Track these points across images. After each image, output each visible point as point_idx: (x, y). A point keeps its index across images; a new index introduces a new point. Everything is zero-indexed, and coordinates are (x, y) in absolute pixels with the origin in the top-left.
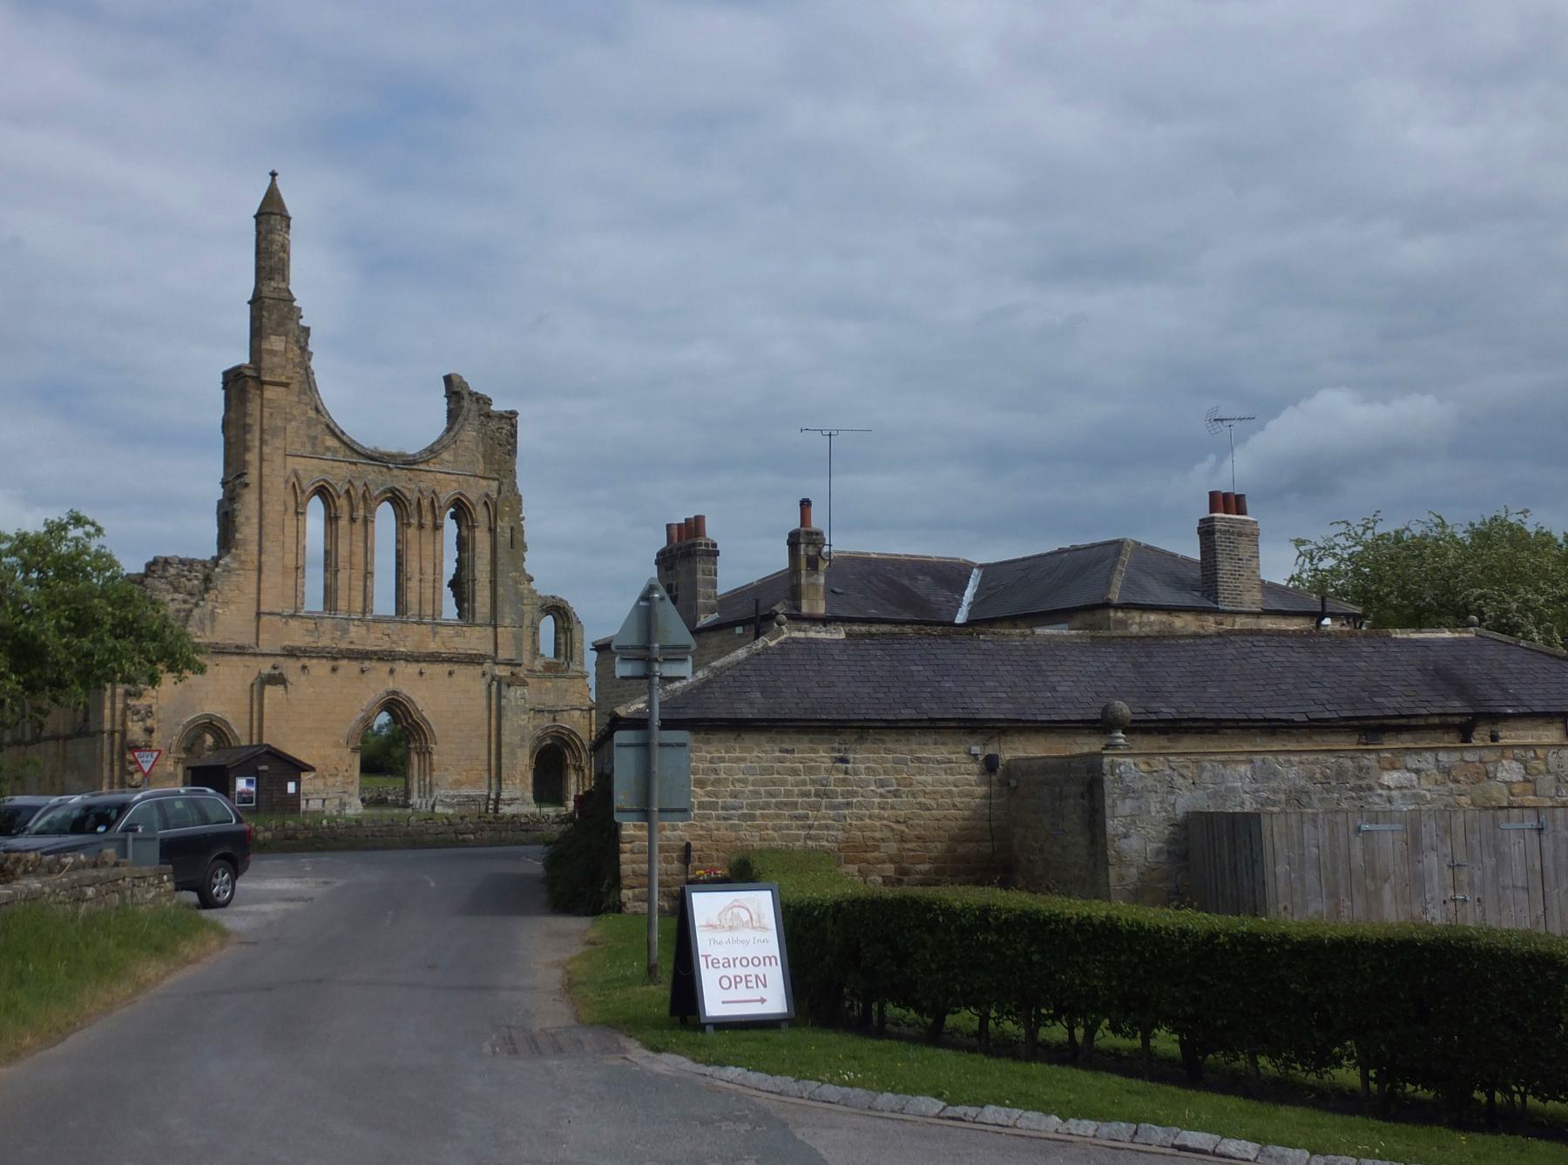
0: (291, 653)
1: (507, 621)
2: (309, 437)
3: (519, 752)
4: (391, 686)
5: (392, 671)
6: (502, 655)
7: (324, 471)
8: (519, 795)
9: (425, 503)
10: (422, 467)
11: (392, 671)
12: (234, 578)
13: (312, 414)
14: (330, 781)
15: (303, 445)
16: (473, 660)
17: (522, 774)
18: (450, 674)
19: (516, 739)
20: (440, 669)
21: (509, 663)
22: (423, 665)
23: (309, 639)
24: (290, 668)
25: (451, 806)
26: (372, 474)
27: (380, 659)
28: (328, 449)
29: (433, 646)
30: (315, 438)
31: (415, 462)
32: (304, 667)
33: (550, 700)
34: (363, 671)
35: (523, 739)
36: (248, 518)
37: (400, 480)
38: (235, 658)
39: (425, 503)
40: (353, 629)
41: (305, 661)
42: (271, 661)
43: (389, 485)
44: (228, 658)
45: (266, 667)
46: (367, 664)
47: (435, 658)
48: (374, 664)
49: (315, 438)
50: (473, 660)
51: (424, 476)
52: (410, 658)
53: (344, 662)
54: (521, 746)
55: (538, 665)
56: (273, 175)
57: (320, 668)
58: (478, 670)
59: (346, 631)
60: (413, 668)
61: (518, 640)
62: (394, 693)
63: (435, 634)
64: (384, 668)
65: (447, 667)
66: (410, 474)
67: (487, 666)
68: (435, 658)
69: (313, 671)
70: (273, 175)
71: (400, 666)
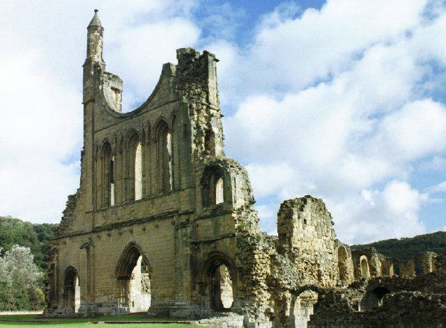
0: (96, 230)
3: (184, 272)
4: (131, 239)
10: (144, 111)
11: (131, 232)
13: (102, 108)
20: (150, 226)
21: (187, 213)
23: (103, 221)
24: (94, 236)
26: (125, 126)
35: (186, 265)
39: (146, 130)
40: (119, 211)
45: (86, 239)
47: (152, 219)
52: (140, 222)
53: (113, 231)
54: (186, 269)
56: (96, 11)
57: (104, 235)
58: (171, 220)
59: (116, 214)
62: (132, 244)
63: (153, 203)
65: (156, 222)
68: (152, 219)
70: (96, 11)
71: (137, 229)
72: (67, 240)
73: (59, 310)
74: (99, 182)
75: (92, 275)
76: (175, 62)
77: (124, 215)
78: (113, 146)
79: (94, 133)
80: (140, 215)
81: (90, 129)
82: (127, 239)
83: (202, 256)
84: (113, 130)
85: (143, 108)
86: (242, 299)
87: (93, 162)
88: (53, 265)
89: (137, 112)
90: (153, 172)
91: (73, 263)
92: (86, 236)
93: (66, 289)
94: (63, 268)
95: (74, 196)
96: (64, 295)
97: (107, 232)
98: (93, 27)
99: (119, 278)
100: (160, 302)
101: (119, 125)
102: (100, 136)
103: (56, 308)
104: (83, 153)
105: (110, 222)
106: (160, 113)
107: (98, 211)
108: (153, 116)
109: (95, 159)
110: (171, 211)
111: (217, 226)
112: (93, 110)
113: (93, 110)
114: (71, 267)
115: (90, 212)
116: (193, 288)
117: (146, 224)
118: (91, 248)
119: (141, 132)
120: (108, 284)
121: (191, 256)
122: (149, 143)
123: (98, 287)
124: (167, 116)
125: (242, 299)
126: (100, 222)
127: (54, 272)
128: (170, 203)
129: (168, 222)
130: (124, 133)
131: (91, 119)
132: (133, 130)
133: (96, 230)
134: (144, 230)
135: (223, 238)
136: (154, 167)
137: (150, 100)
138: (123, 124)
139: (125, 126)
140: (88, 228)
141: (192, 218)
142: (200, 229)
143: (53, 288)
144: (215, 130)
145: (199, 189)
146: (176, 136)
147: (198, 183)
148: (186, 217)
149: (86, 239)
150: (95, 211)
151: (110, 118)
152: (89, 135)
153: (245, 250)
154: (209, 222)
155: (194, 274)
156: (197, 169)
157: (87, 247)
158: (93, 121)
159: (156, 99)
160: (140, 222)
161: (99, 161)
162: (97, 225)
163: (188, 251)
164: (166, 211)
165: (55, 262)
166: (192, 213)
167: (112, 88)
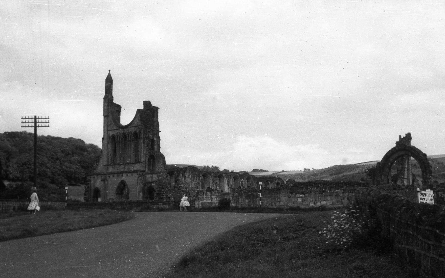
11: (122, 176)
16: (135, 171)
26: (121, 131)
45: (103, 177)
52: (126, 172)
56: (110, 71)
57: (111, 176)
70: (110, 71)
76: (142, 108)
84: (116, 131)
89: (127, 127)
94: (93, 188)
98: (109, 80)
99: (117, 194)
102: (111, 133)
104: (103, 139)
109: (108, 143)
114: (97, 188)
124: (138, 131)
126: (111, 170)
128: (137, 167)
141: (144, 173)
144: (155, 139)
149: (103, 177)
150: (108, 165)
152: (106, 132)
154: (150, 176)
155: (144, 194)
157: (104, 180)
161: (110, 144)
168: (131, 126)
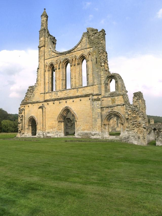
0: (46, 101)
1: (96, 83)
2: (49, 54)
3: (98, 120)
4: (66, 105)
5: (66, 102)
6: (95, 93)
7: (52, 60)
8: (97, 132)
9: (74, 59)
11: (66, 102)
12: (37, 88)
14: (54, 129)
15: (48, 56)
16: (86, 96)
17: (99, 126)
18: (81, 100)
19: (97, 116)
20: (78, 99)
21: (97, 95)
22: (73, 99)
23: (50, 97)
24: (45, 104)
25: (80, 135)
26: (62, 58)
27: (63, 99)
28: (53, 55)
29: (77, 94)
30: (50, 54)
31: (71, 51)
32: (48, 104)
33: (110, 104)
34: (60, 103)
35: (99, 116)
36: (39, 75)
37: (68, 56)
38: (36, 104)
40: (59, 93)
41: (48, 103)
42: (42, 103)
43: (65, 58)
44: (35, 104)
45: (40, 105)
46: (61, 101)
47: (77, 97)
48: (62, 101)
49: (50, 54)
50: (86, 96)
51: (74, 53)
52: (71, 98)
53: (56, 101)
55: (107, 94)
57: (51, 103)
58: (88, 98)
59: (57, 94)
60: (71, 100)
61: (100, 89)
62: (66, 107)
63: (78, 91)
64: (64, 101)
65: (80, 98)
66: (70, 54)
67: (90, 97)
68: (77, 97)
69: (50, 104)
72: (30, 105)
73: (25, 135)
74: (47, 81)
75: (44, 120)
77: (61, 95)
78: (55, 66)
79: (44, 60)
80: (71, 95)
81: (43, 58)
82: (63, 105)
83: (105, 113)
84: (56, 59)
85: (72, 50)
86: (128, 131)
87: (44, 72)
88: (22, 115)
89: (69, 52)
90: (77, 77)
91: (32, 115)
92: (40, 103)
93: (29, 126)
95: (33, 86)
96: (28, 128)
97: (52, 102)
99: (59, 122)
100: (82, 132)
101: (59, 57)
102: (48, 62)
103: (23, 133)
105: (53, 97)
106: (81, 53)
107: (47, 93)
108: (78, 54)
109: (45, 71)
110: (87, 94)
111: (113, 101)
112: (44, 50)
113: (44, 50)
115: (43, 93)
116: (102, 126)
117: (74, 99)
118: (44, 109)
119: (71, 60)
120: (53, 124)
121: (101, 113)
122: (75, 65)
123: (47, 126)
125: (128, 131)
126: (48, 97)
127: (22, 118)
129: (87, 98)
130: (62, 61)
131: (43, 54)
132: (66, 59)
133: (46, 101)
134: (73, 101)
135: (117, 105)
136: (77, 75)
137: (76, 47)
138: (61, 56)
139: (62, 58)
140: (42, 100)
141: (100, 97)
142: (104, 101)
143: (22, 125)
145: (103, 85)
146: (90, 63)
147: (103, 82)
148: (97, 96)
151: (53, 54)
152: (43, 61)
153: (130, 111)
155: (102, 121)
156: (102, 77)
158: (44, 55)
159: (79, 47)
160: (71, 98)
162: (45, 99)
163: (99, 110)
164: (85, 94)
165: (23, 114)
166: (100, 95)
167: (53, 42)
168: (75, 50)
